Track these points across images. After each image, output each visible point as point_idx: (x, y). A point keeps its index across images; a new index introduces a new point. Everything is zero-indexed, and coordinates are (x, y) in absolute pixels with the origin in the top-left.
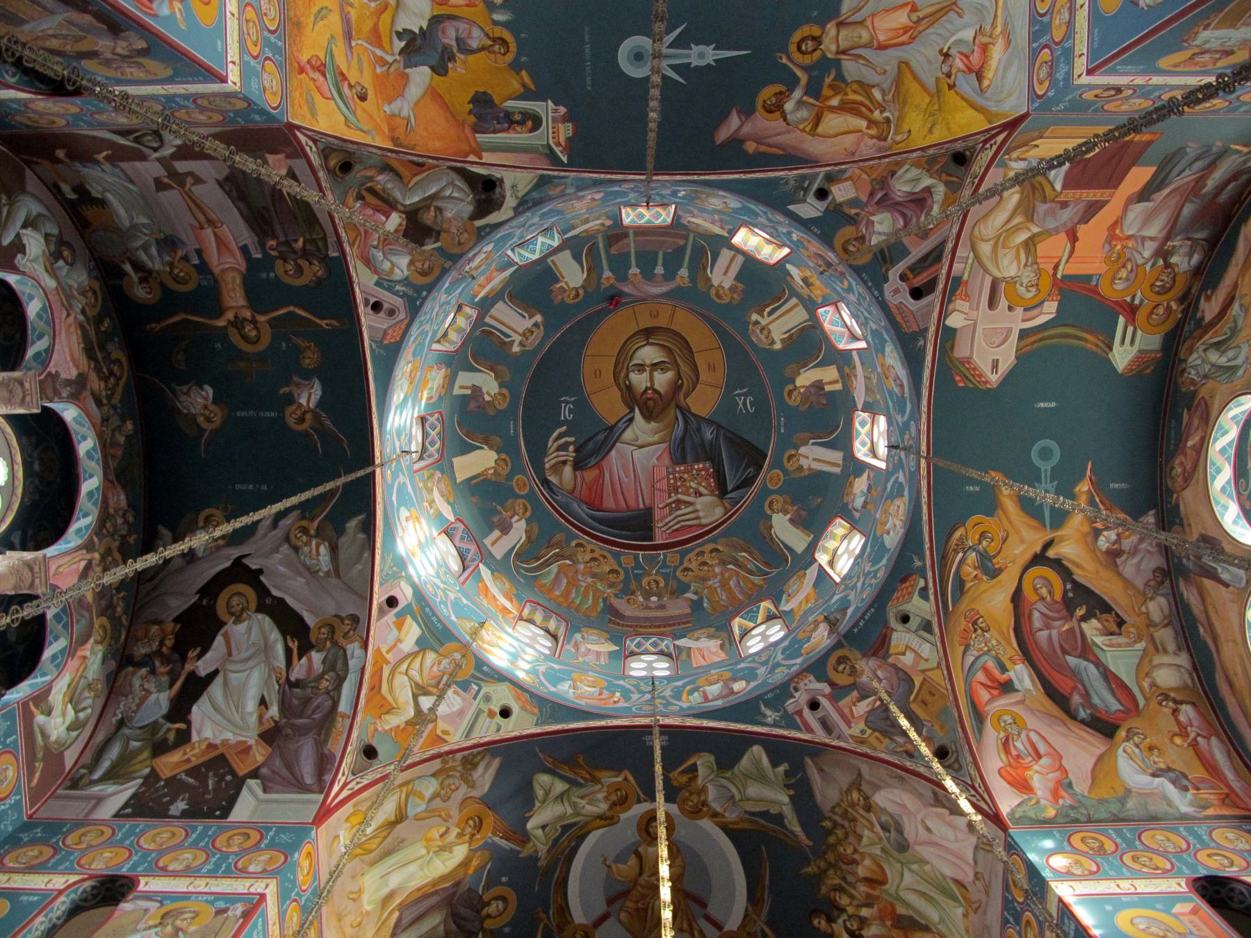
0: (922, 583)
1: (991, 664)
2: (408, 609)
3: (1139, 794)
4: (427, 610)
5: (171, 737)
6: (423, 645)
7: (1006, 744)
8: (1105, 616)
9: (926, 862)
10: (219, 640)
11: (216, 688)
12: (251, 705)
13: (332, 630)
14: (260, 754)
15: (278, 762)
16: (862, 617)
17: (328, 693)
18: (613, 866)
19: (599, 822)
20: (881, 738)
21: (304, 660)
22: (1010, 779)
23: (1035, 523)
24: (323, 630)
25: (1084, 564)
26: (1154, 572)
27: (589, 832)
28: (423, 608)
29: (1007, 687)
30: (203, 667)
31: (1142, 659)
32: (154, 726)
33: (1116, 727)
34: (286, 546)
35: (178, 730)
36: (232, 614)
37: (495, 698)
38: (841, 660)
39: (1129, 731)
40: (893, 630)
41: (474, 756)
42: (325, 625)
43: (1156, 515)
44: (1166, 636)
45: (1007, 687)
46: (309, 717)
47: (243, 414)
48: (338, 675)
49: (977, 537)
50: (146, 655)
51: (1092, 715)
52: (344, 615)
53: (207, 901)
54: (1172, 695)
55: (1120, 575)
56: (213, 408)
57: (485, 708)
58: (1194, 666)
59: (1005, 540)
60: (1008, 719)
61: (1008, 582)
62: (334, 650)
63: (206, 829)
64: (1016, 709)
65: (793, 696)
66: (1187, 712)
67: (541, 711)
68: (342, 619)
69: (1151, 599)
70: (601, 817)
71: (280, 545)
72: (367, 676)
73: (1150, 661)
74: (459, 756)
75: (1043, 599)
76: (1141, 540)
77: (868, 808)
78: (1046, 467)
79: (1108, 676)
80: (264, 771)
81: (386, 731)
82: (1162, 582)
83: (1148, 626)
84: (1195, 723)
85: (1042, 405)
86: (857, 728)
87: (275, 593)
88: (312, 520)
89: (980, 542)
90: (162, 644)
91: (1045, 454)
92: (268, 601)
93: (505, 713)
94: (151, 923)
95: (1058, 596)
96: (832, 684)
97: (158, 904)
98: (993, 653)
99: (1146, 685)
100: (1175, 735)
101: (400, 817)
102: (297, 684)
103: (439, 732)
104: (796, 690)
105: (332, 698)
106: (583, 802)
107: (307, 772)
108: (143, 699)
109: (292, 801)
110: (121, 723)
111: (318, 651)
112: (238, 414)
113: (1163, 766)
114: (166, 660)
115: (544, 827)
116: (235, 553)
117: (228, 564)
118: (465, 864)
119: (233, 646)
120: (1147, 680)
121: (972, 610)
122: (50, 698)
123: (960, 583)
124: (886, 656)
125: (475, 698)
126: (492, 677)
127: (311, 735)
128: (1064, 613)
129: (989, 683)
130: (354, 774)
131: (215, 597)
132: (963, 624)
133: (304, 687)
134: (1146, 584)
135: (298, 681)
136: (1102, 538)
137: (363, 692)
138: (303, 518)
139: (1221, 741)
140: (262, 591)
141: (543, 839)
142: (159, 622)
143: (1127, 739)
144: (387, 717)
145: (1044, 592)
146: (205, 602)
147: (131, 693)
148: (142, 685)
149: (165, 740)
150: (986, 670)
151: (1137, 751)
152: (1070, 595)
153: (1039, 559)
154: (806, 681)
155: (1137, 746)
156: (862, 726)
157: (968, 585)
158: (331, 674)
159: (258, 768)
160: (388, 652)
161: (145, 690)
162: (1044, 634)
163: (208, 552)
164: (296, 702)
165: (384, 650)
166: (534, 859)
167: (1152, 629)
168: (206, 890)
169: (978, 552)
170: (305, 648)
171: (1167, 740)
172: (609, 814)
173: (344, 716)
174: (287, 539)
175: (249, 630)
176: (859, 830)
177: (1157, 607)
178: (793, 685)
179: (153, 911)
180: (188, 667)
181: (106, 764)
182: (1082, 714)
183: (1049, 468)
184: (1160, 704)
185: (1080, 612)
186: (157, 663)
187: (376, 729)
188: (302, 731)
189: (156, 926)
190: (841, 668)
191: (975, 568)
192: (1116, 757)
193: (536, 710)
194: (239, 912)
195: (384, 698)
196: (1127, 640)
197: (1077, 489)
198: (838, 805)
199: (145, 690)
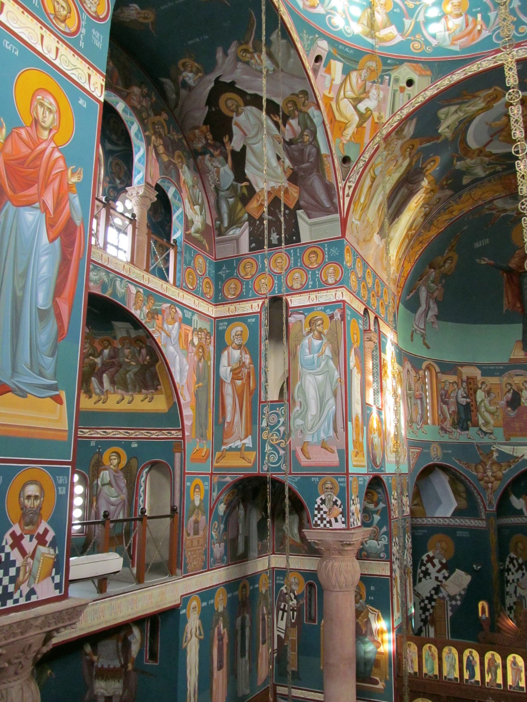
2: (330, 56)
4: (340, 47)
5: (245, 191)
6: (346, 72)
10: (235, 128)
11: (249, 156)
12: (274, 162)
13: (295, 104)
14: (294, 192)
15: (306, 195)
17: (311, 143)
18: (492, 124)
19: (481, 111)
21: (287, 126)
24: (289, 105)
27: (474, 118)
28: (337, 48)
30: (236, 145)
32: (232, 188)
34: (240, 64)
35: (246, 186)
36: (233, 111)
37: (400, 77)
41: (401, 127)
42: (289, 101)
46: (308, 162)
47: (165, 7)
48: (311, 131)
50: (203, 147)
52: (297, 92)
53: (321, 310)
56: (143, 12)
57: (397, 87)
62: (301, 116)
63: (295, 251)
67: (432, 72)
68: (297, 95)
70: (482, 109)
71: (236, 65)
72: (327, 122)
74: (393, 134)
80: (302, 203)
81: (348, 141)
87: (249, 92)
88: (247, 43)
90: (206, 139)
92: (248, 98)
93: (410, 83)
94: (308, 329)
97: (303, 316)
101: (373, 179)
102: (290, 143)
103: (376, 121)
105: (315, 146)
106: (469, 108)
107: (323, 197)
108: (218, 172)
109: (325, 222)
110: (217, 189)
111: (293, 118)
112: (162, 8)
114: (216, 148)
115: (448, 127)
116: (212, 77)
117: (212, 85)
118: (410, 164)
119: (245, 130)
122: (189, 218)
125: (389, 85)
126: (396, 65)
127: (314, 173)
130: (344, 180)
131: (217, 105)
133: (296, 143)
135: (290, 140)
137: (328, 127)
138: (241, 44)
140: (242, 94)
141: (449, 131)
142: (197, 128)
144: (346, 132)
146: (213, 109)
147: (210, 171)
148: (212, 165)
149: (243, 194)
158: (307, 131)
159: (298, 202)
160: (329, 93)
161: (215, 167)
163: (196, 82)
164: (296, 154)
165: (327, 93)
166: (446, 139)
168: (317, 302)
170: (285, 119)
172: (487, 106)
173: (326, 156)
174: (238, 59)
175: (248, 118)
179: (303, 321)
180: (229, 148)
181: (225, 216)
186: (211, 150)
187: (343, 144)
188: (308, 172)
189: (310, 332)
193: (429, 73)
194: (339, 317)
195: (339, 122)
199: (215, 167)
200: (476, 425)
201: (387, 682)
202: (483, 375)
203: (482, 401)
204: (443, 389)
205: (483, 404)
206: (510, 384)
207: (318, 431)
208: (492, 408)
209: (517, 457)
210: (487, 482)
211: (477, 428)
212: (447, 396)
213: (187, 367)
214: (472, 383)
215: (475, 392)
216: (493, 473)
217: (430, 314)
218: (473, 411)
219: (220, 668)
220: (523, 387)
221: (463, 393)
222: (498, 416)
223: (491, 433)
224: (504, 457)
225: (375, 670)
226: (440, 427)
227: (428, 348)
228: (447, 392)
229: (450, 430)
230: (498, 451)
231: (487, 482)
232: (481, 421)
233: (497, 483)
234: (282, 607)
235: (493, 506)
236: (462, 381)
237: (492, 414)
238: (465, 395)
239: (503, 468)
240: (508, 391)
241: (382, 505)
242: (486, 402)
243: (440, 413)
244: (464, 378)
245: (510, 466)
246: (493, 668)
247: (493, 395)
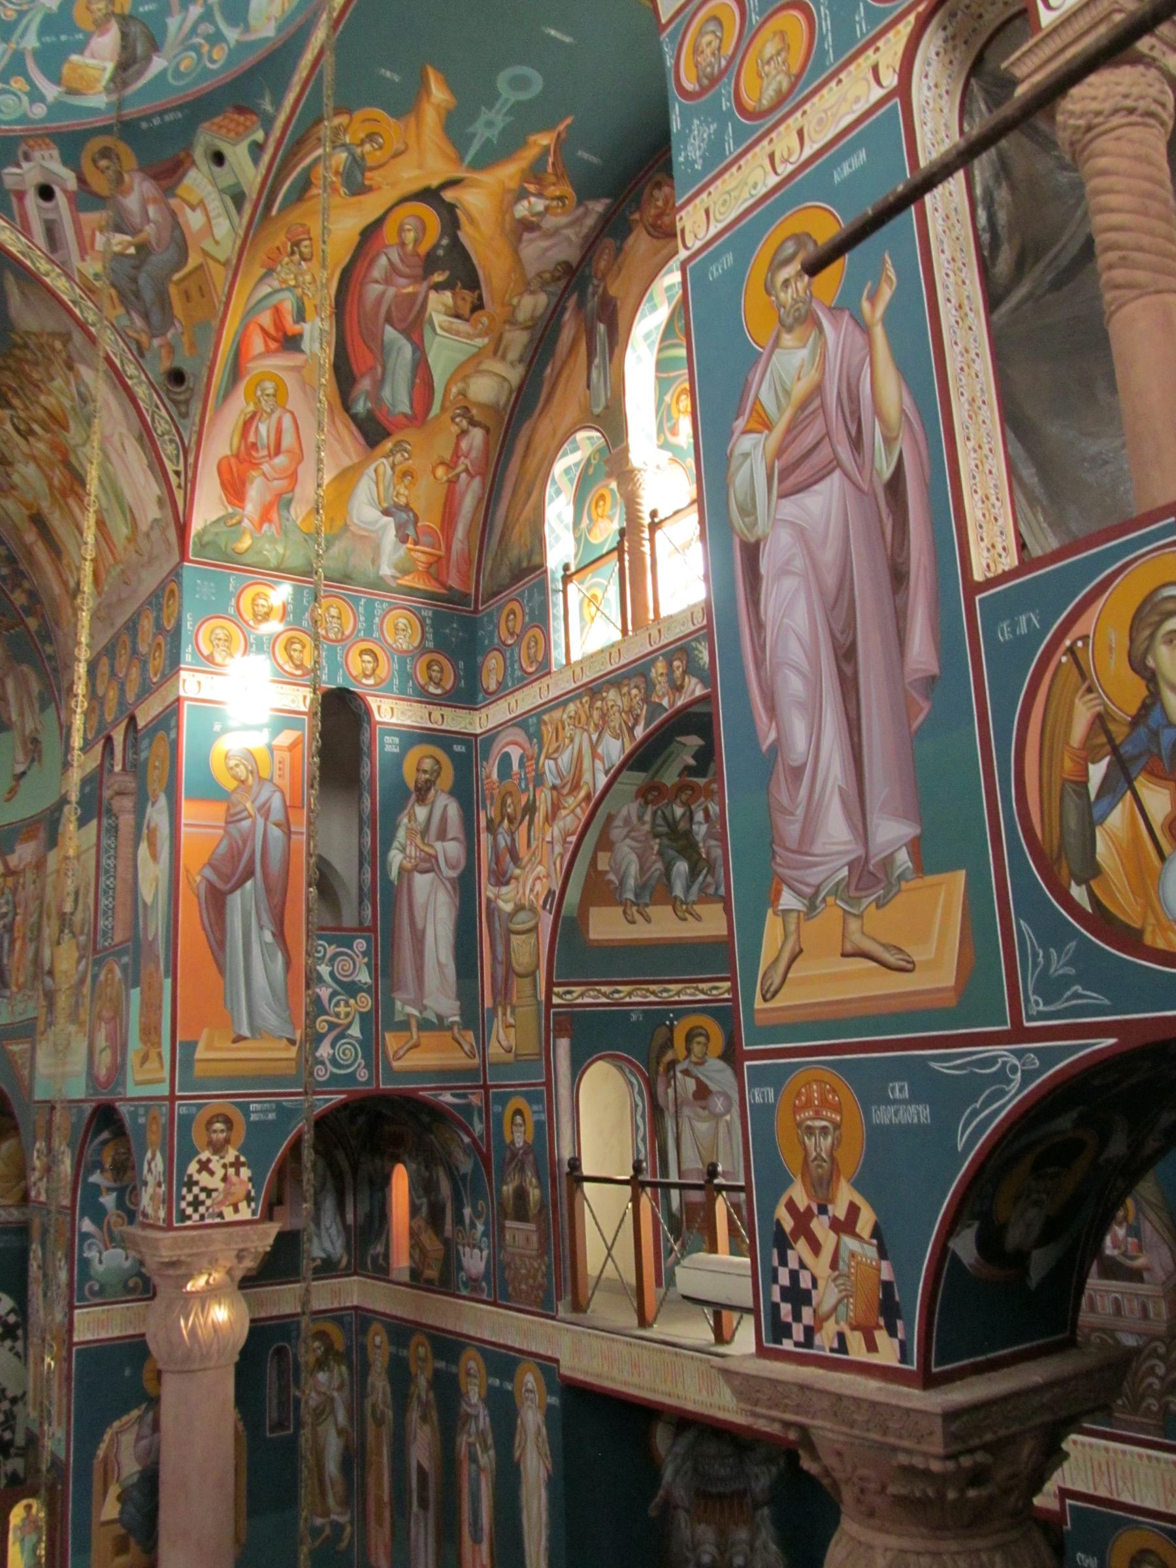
0: (259, 136)
1: (288, 304)
3: (354, 535)
7: (248, 424)
8: (466, 293)
9: (111, 463)
16: (161, 114)
20: (116, 301)
22: (227, 476)
23: (449, 150)
25: (483, 227)
26: (559, 264)
29: (290, 343)
31: (474, 356)
33: (387, 434)
38: (106, 153)
39: (395, 445)
40: (193, 163)
43: (608, 208)
44: (517, 340)
45: (290, 343)
49: (362, 135)
51: (370, 412)
54: (474, 411)
55: (516, 252)
58: (520, 388)
59: (397, 155)
60: (269, 387)
61: (370, 208)
64: (283, 375)
65: (18, 166)
66: (477, 434)
69: (533, 293)
73: (479, 363)
75: (403, 244)
76: (570, 225)
77: (71, 368)
78: (508, 96)
79: (421, 367)
82: (559, 279)
83: (505, 322)
84: (473, 454)
85: (553, 32)
86: (92, 267)
89: (362, 143)
91: (519, 83)
95: (423, 249)
96: (81, 180)
98: (299, 291)
99: (454, 390)
100: (442, 463)
104: (27, 158)
113: (403, 501)
120: (460, 385)
121: (303, 225)
123: (304, 186)
124: (169, 191)
128: (419, 271)
129: (272, 331)
132: (281, 240)
134: (539, 275)
136: (525, 203)
139: (483, 488)
143: (386, 456)
145: (410, 237)
150: (277, 311)
151: (389, 471)
152: (441, 252)
153: (429, 195)
154: (46, 154)
155: (393, 467)
156: (98, 267)
157: (314, 191)
162: (378, 288)
167: (507, 327)
169: (352, 154)
171: (429, 468)
176: (52, 371)
177: (532, 304)
178: (23, 147)
182: (360, 407)
183: (513, 100)
184: (453, 419)
185: (438, 277)
190: (103, 163)
191: (337, 173)
192: (361, 475)
196: (471, 331)
197: (532, 138)
198: (35, 334)
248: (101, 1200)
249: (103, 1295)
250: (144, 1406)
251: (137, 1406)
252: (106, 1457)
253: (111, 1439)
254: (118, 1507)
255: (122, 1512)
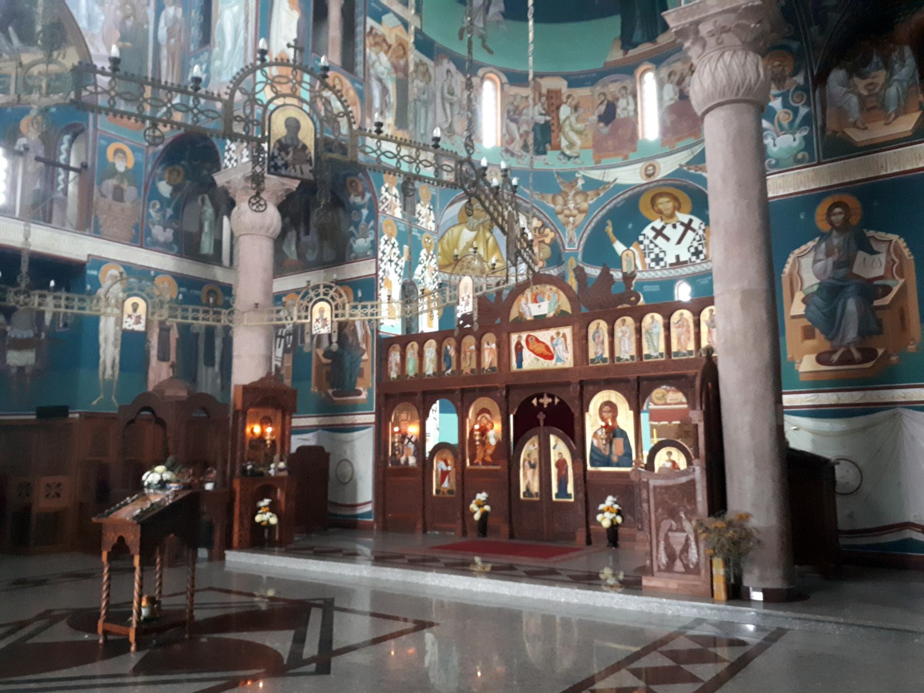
200: (558, 147)
201: (370, 392)
202: (570, 85)
203: (567, 118)
204: (512, 103)
205: (567, 122)
206: (604, 94)
207: (232, 68)
208: (580, 126)
209: (608, 183)
210: (568, 216)
211: (559, 152)
212: (517, 112)
213: (103, 18)
214: (554, 97)
215: (558, 108)
216: (576, 204)
217: (492, 10)
218: (553, 131)
219: (163, 356)
220: (619, 95)
221: (541, 109)
222: (586, 135)
223: (577, 157)
224: (592, 185)
225: (359, 380)
226: (503, 148)
227: (491, 52)
228: (517, 108)
229: (519, 154)
230: (584, 177)
231: (568, 216)
232: (564, 143)
233: (581, 217)
234: (280, 334)
235: (575, 244)
236: (541, 95)
237: (579, 133)
238: (544, 112)
239: (589, 198)
240: (602, 103)
241: (368, 196)
242: (573, 119)
243: (504, 131)
244: (544, 91)
245: (598, 194)
246: (468, 354)
247: (581, 111)
248: (771, 104)
249: (781, 167)
250: (817, 239)
251: (812, 239)
252: (791, 274)
253: (794, 260)
254: (803, 307)
255: (806, 311)
